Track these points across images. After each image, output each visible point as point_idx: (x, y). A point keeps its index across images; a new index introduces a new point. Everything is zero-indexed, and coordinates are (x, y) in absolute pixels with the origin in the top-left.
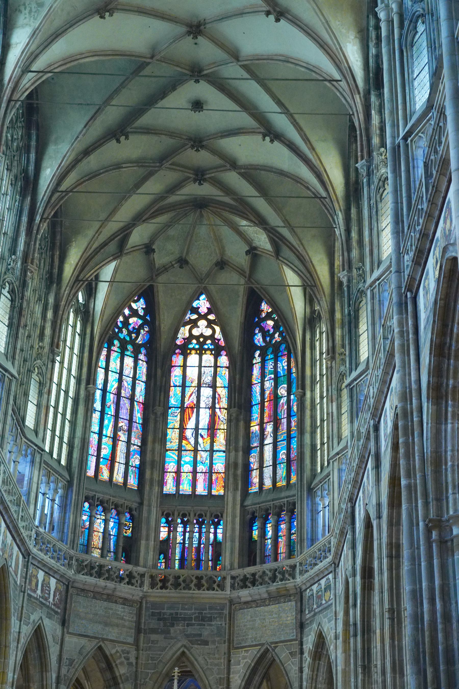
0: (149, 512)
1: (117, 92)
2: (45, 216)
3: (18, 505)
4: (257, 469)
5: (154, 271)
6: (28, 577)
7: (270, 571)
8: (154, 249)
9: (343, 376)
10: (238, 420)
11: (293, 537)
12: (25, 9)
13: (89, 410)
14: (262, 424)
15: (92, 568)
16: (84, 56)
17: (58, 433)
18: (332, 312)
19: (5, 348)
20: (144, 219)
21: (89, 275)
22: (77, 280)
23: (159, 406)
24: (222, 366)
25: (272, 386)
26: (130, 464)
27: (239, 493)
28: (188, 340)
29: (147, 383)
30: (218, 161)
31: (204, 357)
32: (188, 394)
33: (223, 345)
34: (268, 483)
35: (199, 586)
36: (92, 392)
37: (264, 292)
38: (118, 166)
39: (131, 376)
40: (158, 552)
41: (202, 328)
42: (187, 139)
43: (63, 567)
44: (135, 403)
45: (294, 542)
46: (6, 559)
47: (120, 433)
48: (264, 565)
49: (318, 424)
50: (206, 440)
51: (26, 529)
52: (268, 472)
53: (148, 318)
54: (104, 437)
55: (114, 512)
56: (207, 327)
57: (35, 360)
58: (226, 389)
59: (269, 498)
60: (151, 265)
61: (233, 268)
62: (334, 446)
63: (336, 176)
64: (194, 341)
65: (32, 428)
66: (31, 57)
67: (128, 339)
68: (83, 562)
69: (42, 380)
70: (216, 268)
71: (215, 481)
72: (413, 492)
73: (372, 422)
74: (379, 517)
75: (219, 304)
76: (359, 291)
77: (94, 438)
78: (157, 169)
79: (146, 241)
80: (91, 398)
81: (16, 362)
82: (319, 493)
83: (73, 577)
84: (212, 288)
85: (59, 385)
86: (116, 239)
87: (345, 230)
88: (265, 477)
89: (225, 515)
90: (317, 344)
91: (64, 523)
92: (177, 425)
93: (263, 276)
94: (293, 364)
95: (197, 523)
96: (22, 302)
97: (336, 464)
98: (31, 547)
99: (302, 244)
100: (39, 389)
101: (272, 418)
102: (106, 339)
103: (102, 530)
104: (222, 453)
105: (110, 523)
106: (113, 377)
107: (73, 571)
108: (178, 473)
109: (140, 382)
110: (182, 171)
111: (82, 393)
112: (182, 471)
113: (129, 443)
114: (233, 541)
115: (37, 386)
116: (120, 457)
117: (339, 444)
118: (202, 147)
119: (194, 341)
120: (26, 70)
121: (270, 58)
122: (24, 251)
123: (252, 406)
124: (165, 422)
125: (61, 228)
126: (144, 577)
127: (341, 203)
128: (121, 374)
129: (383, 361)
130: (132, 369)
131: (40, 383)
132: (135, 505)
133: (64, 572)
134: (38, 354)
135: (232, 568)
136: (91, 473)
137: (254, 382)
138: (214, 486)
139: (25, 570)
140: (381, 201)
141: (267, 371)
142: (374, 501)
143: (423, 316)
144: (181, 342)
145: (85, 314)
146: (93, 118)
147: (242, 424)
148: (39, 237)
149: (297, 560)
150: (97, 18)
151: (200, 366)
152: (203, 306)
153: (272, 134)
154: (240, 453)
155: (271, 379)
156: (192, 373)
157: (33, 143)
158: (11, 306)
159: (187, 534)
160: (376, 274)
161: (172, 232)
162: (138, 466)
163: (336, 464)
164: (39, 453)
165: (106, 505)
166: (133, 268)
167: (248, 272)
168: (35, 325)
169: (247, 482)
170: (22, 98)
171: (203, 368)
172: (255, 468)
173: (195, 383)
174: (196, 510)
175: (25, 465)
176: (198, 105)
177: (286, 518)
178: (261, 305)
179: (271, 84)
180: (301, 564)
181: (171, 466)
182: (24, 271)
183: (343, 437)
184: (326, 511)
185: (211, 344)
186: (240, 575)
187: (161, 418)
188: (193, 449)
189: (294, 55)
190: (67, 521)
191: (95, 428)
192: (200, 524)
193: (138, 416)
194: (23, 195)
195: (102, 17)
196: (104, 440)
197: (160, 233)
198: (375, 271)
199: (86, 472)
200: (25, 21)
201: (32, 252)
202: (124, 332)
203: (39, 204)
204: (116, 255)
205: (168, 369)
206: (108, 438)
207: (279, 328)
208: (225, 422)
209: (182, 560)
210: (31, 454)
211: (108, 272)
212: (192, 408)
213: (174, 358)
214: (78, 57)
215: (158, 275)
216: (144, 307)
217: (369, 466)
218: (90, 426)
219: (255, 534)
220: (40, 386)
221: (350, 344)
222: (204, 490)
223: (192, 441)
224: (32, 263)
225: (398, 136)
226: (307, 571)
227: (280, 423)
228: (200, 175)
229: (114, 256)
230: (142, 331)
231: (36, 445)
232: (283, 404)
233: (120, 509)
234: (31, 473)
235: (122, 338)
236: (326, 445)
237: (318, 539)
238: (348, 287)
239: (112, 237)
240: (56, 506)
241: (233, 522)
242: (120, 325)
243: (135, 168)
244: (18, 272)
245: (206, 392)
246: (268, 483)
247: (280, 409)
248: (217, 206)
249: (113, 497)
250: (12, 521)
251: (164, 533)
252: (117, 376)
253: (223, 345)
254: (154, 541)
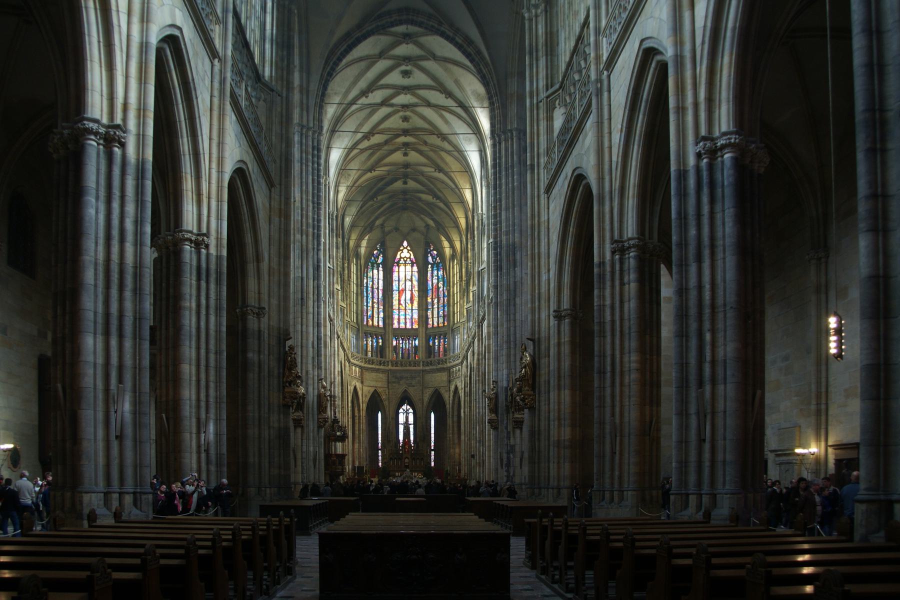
5: (385, 234)
34: (436, 324)
35: (410, 365)
38: (372, 205)
52: (436, 320)
60: (383, 232)
108: (399, 319)
113: (378, 308)
116: (376, 315)
124: (392, 298)
166: (377, 234)
169: (427, 323)
181: (396, 317)
184: (460, 341)
193: (380, 295)
245: (409, 283)
246: (436, 324)
251: (394, 343)
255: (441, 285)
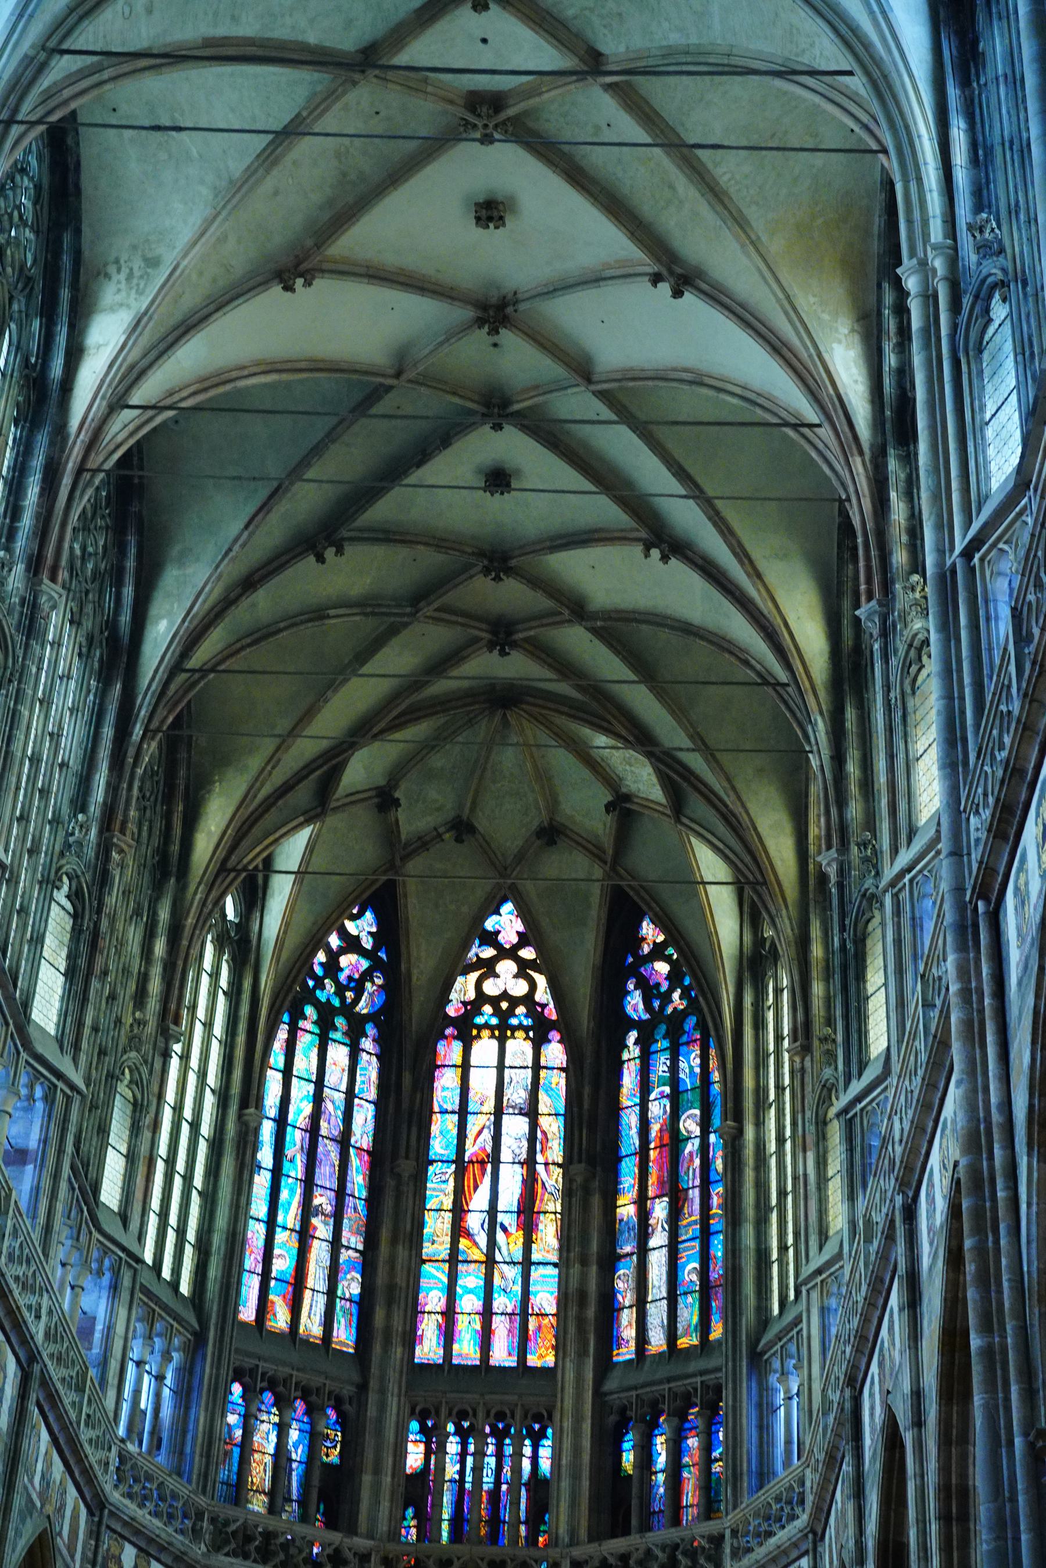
0: (382, 1406)
1: (317, 451)
2: (154, 725)
3: (80, 1389)
4: (631, 1307)
5: (397, 850)
6: (100, 1559)
7: (663, 1548)
8: (398, 800)
9: (830, 1091)
10: (587, 1192)
11: (717, 1467)
12: (119, 271)
13: (247, 1167)
14: (642, 1202)
15: (249, 1539)
16: (246, 372)
17: (173, 1220)
18: (803, 942)
19: (58, 1025)
20: (375, 730)
21: (252, 858)
22: (223, 869)
23: (407, 1157)
24: (550, 1065)
25: (665, 1112)
26: (339, 1293)
27: (590, 1362)
28: (473, 1007)
29: (379, 1104)
30: (542, 602)
31: (510, 1044)
32: (472, 1130)
33: (554, 1017)
34: (657, 1340)
36: (253, 1125)
37: (647, 897)
38: (318, 614)
39: (343, 1087)
40: (401, 1503)
41: (506, 979)
42: (473, 554)
43: (180, 1538)
44: (352, 1151)
45: (719, 1478)
46: (49, 1517)
47: (315, 1221)
48: (650, 1534)
49: (774, 1202)
50: (511, 1239)
51: (96, 1447)
52: (657, 1314)
53: (382, 955)
54: (278, 1230)
55: (299, 1405)
56: (516, 976)
57: (125, 1052)
58: (561, 1119)
59: (658, 1376)
60: (390, 836)
61: (578, 843)
62: (811, 1254)
63: (810, 635)
64: (488, 1009)
65: (116, 1210)
66: (129, 375)
67: (336, 1002)
68: (227, 1523)
69: (139, 1096)
70: (538, 842)
71: (535, 1333)
72: (998, 1366)
73: (899, 1200)
74: (918, 1423)
75: (545, 922)
76: (864, 895)
77: (256, 1233)
78: (405, 619)
79: (382, 782)
80: (251, 1138)
81: (83, 1058)
82: (776, 1364)
83: (203, 1561)
84: (529, 887)
85: (178, 1109)
86: (312, 777)
87: (832, 758)
88: (649, 1326)
89: (557, 1416)
90: (770, 1015)
91: (184, 1432)
92: (448, 1203)
93: (646, 861)
94: (713, 1063)
95: (492, 1434)
96: (99, 919)
97: (815, 1295)
98: (108, 1488)
99: (733, 788)
100: (133, 1118)
101: (667, 1187)
102: (287, 1004)
103: (271, 1450)
104: (550, 1267)
105: (291, 1432)
106: (301, 1093)
107: (203, 1546)
108: (449, 1314)
109: (363, 1102)
110: (462, 625)
111: (231, 1127)
112: (458, 1310)
113: (336, 1244)
114: (576, 1477)
115: (129, 1112)
116: (316, 1277)
117: (821, 1249)
118: (509, 571)
119: (488, 1009)
120: (118, 403)
121: (661, 376)
122: (105, 803)
123: (620, 1159)
125: (189, 752)
126: (369, 1561)
127: (822, 694)
128: (319, 1083)
129: (923, 1057)
130: (346, 1073)
131: (135, 1104)
132: (347, 1391)
133: (183, 1549)
134: (131, 1039)
135: (574, 1542)
136: (248, 1313)
137: (625, 1102)
138: (531, 1345)
139: (93, 1542)
140: (914, 693)
141: (653, 1078)
142: (906, 1387)
143: (1014, 955)
144: (457, 1010)
145: (240, 945)
146: (265, 507)
147: (596, 1201)
148: (139, 771)
149: (726, 1522)
150: (277, 290)
151: (501, 1067)
152: (508, 928)
153: (665, 541)
154: (594, 1269)
155: (662, 1095)
156: (483, 1083)
157: (130, 564)
158: (73, 929)
159: (470, 1460)
160: (905, 858)
161: (438, 761)
162: (357, 1299)
163: (815, 1295)
164: (130, 1266)
165: (281, 1389)
167: (610, 852)
168: (126, 971)
169: (608, 1338)
170: (108, 466)
171: (507, 1071)
172: (627, 1304)
173: (490, 1106)
174: (489, 1400)
175: (95, 1295)
176: (498, 479)
177: (700, 1423)
178: (639, 926)
179: (662, 433)
180: (735, 1533)
181: (433, 1299)
182: (105, 848)
183: (831, 1233)
184: (793, 1405)
185: (526, 1016)
186: (591, 1558)
187: (412, 1187)
188: (483, 1258)
189: (716, 371)
190: (191, 1427)
191: (259, 1208)
192: (500, 1436)
193: (358, 1180)
194: (105, 678)
195: (289, 288)
196: (281, 1236)
197: (412, 763)
198: (902, 851)
199: (236, 1312)
200: (118, 298)
201: (122, 806)
202: (328, 986)
203: (140, 697)
204: (312, 813)
205: (427, 1071)
206: (288, 1232)
207: (683, 980)
208: (558, 1195)
209: (457, 1520)
210: (112, 1268)
211: (293, 850)
212: (482, 1163)
213: (441, 1047)
214: (234, 374)
215: (405, 858)
216: (374, 929)
217: (894, 1301)
218: (248, 1203)
219: (628, 1459)
220: (134, 1111)
221: (846, 1017)
222: (510, 1354)
223: (482, 1240)
224: (123, 831)
225: (952, 549)
226: (750, 1550)
227: (686, 1199)
228: (502, 634)
229: (307, 816)
230: (368, 985)
231: (124, 1249)
232: (691, 1154)
233: (313, 1398)
234: (112, 1312)
235: (324, 1000)
236: (791, 1251)
237: (775, 1474)
238: (840, 886)
239: (304, 773)
240: (166, 1392)
241: (577, 1432)
242: (319, 971)
243: (357, 618)
244: (90, 853)
245: (515, 1127)
246: (657, 1340)
247: (686, 1165)
248: (540, 702)
249: (298, 1370)
250: (64, 1428)
251: (415, 1457)
252: (311, 1087)
253: (554, 1017)
254: (393, 1476)
255: (689, 1124)
